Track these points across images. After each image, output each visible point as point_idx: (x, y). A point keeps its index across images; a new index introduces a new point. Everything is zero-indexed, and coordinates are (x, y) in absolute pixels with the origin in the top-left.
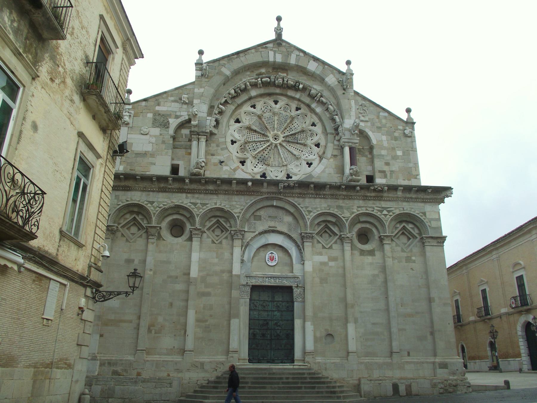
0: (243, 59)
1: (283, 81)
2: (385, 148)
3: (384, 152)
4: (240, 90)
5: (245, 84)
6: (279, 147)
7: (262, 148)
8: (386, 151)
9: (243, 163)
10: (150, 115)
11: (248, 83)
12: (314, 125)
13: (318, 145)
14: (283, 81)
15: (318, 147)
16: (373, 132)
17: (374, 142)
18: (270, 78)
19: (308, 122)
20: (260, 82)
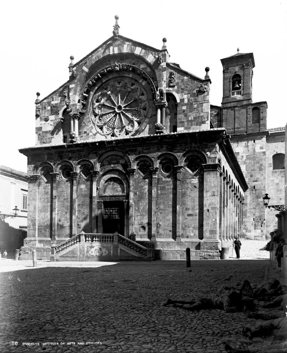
0: (94, 57)
1: (120, 67)
2: (185, 105)
3: (184, 108)
4: (95, 80)
5: (98, 76)
6: (121, 114)
7: (112, 117)
8: (186, 106)
9: (101, 128)
10: (49, 108)
11: (99, 75)
12: (143, 94)
13: (145, 109)
14: (120, 67)
15: (145, 110)
16: (178, 93)
17: (178, 101)
18: (111, 67)
19: (138, 94)
20: (106, 71)
